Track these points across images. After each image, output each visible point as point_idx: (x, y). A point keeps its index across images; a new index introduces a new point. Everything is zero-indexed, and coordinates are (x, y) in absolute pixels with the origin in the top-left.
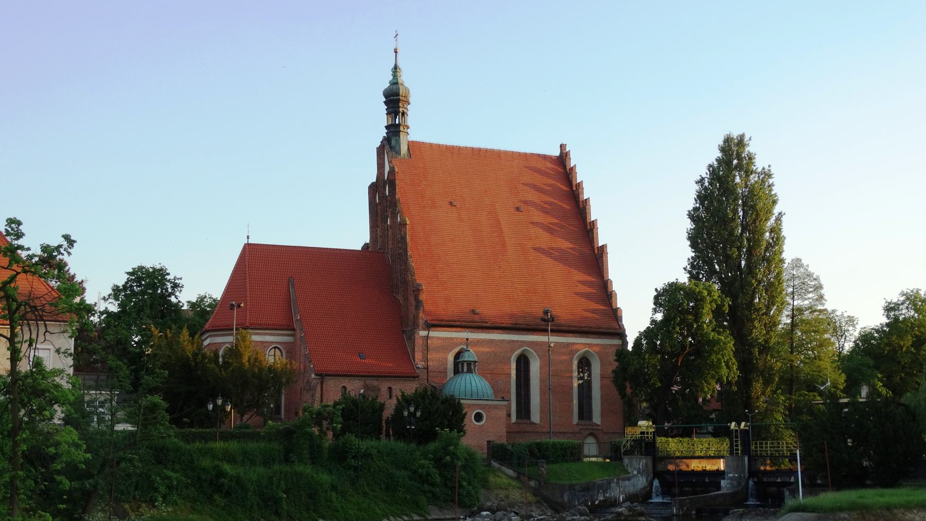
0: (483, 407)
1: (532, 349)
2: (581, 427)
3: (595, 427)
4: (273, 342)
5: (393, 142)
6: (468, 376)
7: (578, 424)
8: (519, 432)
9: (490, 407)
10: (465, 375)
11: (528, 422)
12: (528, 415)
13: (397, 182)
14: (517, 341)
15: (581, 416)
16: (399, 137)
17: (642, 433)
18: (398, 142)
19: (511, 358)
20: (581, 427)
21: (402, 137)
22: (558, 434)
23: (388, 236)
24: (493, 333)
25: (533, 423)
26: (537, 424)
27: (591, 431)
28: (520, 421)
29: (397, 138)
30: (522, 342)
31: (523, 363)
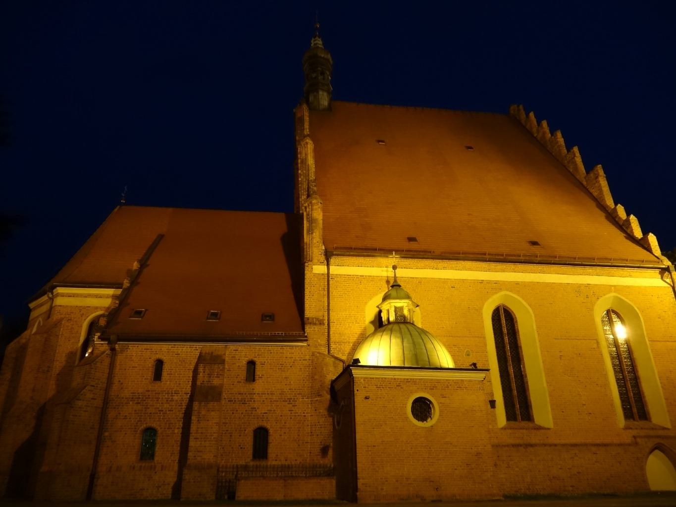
0: (433, 386)
1: (518, 293)
2: (634, 432)
4: (96, 308)
8: (513, 446)
9: (447, 384)
10: (390, 326)
14: (489, 282)
16: (318, 92)
19: (481, 308)
21: (321, 93)
22: (594, 449)
24: (444, 268)
25: (540, 428)
26: (549, 429)
28: (512, 423)
29: (315, 93)
30: (496, 283)
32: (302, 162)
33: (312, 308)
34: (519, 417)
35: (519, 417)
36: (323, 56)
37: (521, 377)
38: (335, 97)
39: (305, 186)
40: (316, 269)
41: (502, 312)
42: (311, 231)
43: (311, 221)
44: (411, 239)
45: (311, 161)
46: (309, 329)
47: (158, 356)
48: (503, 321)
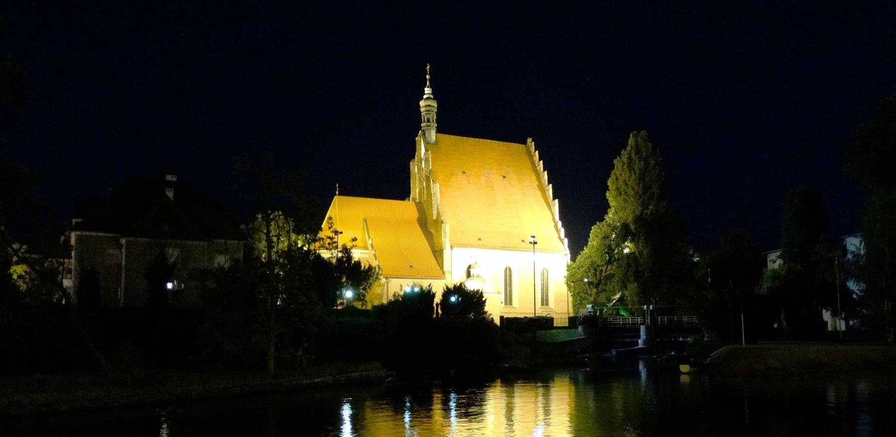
2: (542, 310)
3: (551, 310)
5: (427, 134)
6: (477, 278)
7: (541, 308)
10: (475, 278)
11: (511, 306)
12: (511, 304)
13: (430, 159)
15: (542, 304)
16: (431, 131)
17: (589, 312)
18: (430, 134)
20: (542, 310)
21: (432, 131)
23: (424, 193)
25: (514, 308)
27: (548, 312)
31: (508, 273)
32: (434, 194)
33: (446, 267)
34: (508, 304)
35: (508, 304)
36: (433, 105)
37: (511, 291)
38: (439, 130)
39: (436, 206)
40: (447, 253)
41: (508, 269)
42: (445, 236)
43: (445, 233)
44: (480, 239)
45: (438, 194)
46: (446, 275)
47: (400, 284)
48: (508, 272)
